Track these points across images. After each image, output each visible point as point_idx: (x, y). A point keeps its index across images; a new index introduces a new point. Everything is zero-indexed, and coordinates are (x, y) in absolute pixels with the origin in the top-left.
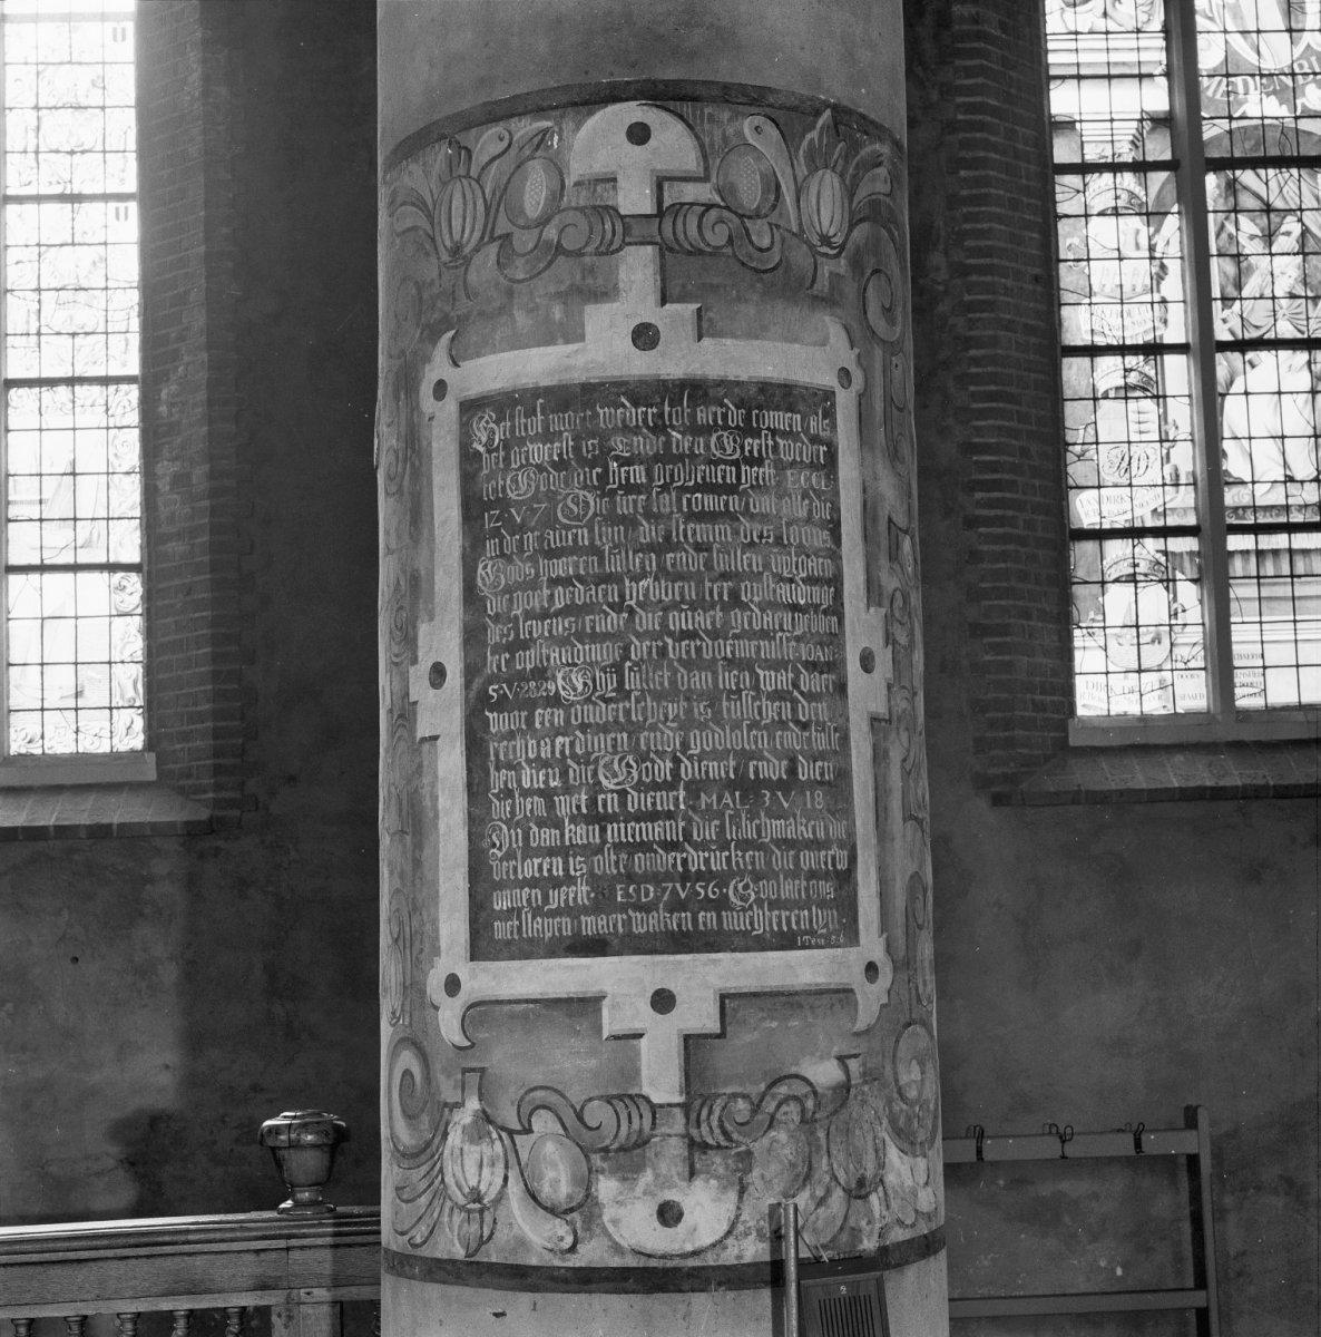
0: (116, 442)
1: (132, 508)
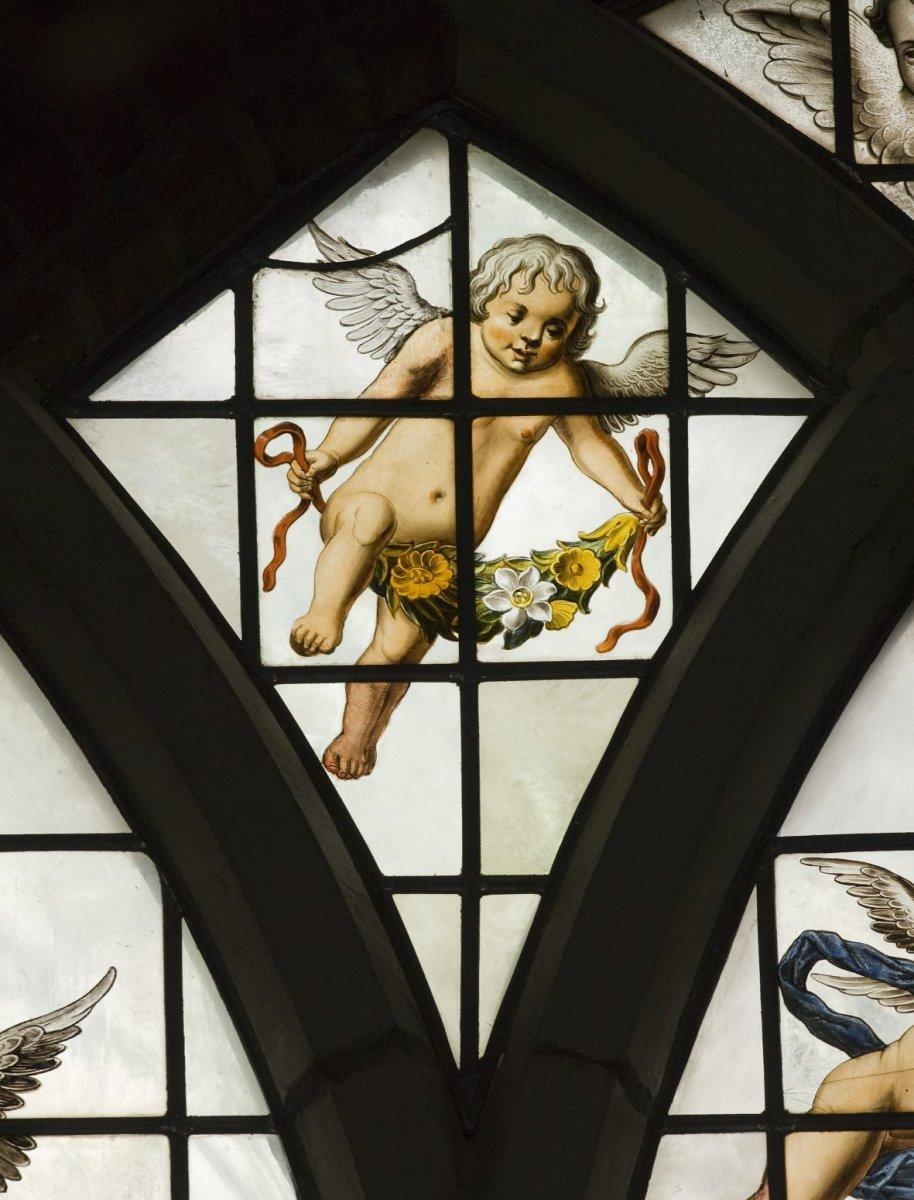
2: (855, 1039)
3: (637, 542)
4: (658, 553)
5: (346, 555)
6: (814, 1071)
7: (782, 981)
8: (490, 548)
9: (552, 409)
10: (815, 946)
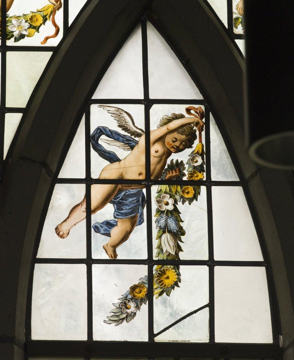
2: (112, 158)
3: (53, 13)
4: (59, 16)
6: (100, 167)
7: (92, 141)
10: (101, 131)
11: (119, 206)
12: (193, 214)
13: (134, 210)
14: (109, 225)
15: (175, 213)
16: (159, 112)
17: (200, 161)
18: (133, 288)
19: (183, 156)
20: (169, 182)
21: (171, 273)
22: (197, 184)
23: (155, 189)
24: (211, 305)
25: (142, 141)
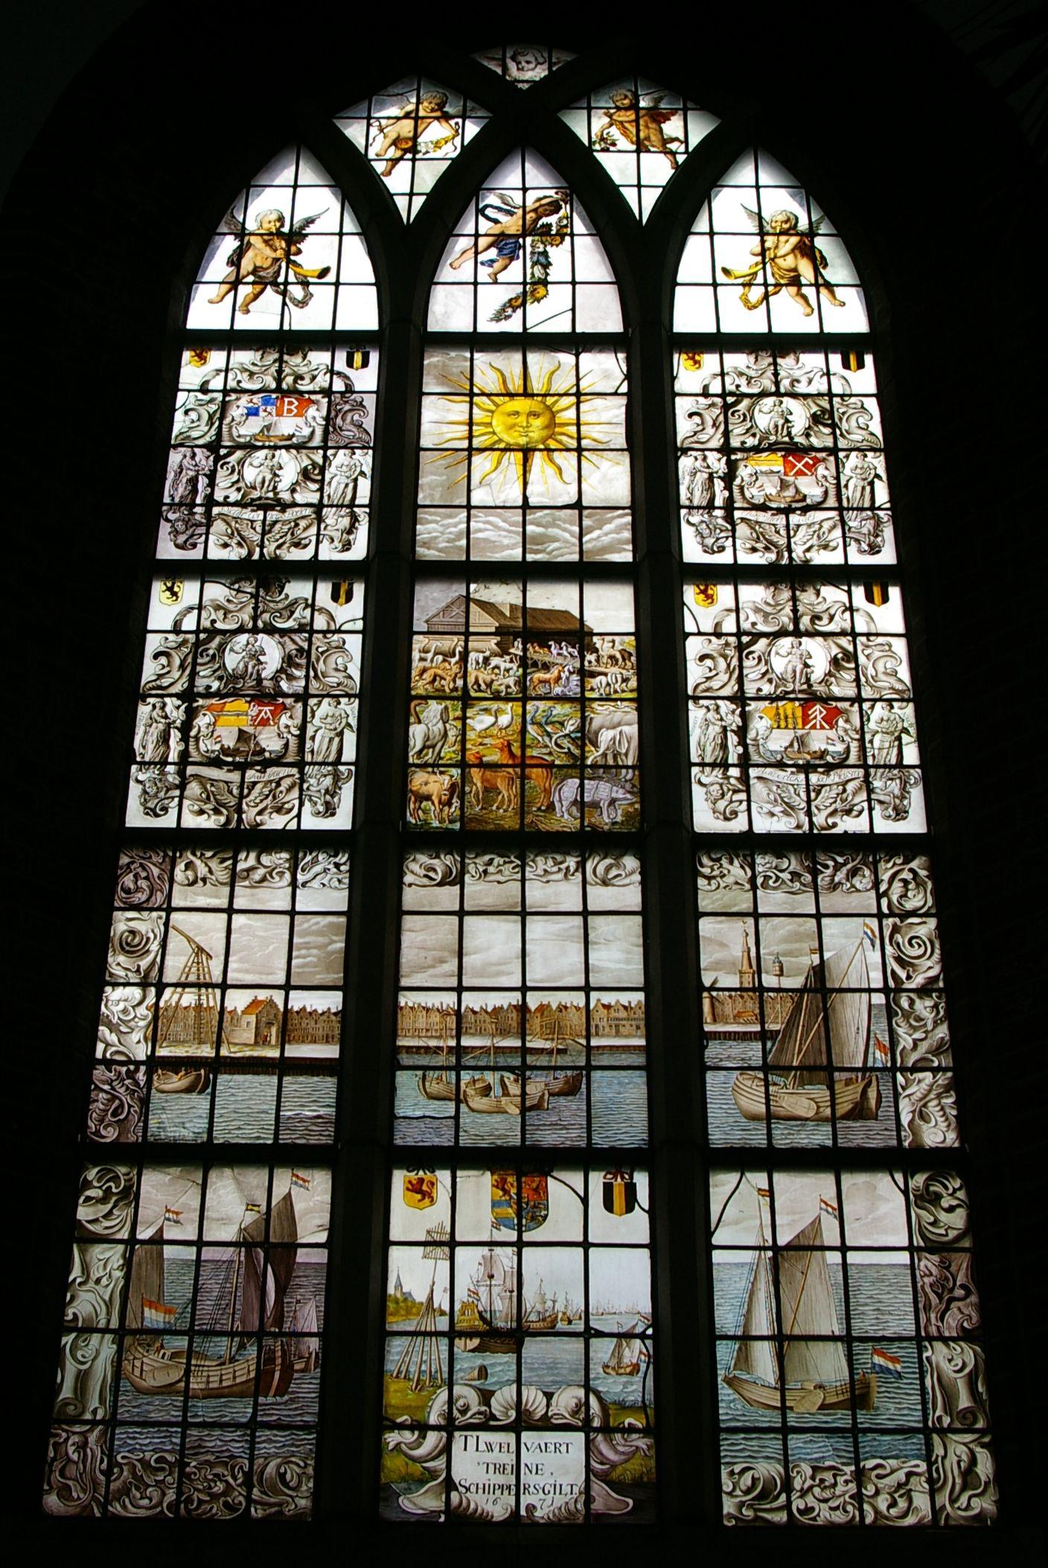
0: (898, 937)
1: (937, 1051)
2: (496, 221)
5: (389, 141)
6: (485, 226)
8: (419, 140)
9: (437, 118)
11: (500, 250)
12: (559, 255)
13: (514, 252)
14: (493, 261)
15: (545, 254)
16: (532, 196)
17: (565, 222)
18: (510, 300)
19: (552, 219)
20: (541, 235)
21: (541, 290)
22: (562, 236)
23: (529, 240)
24: (573, 310)
25: (520, 212)
